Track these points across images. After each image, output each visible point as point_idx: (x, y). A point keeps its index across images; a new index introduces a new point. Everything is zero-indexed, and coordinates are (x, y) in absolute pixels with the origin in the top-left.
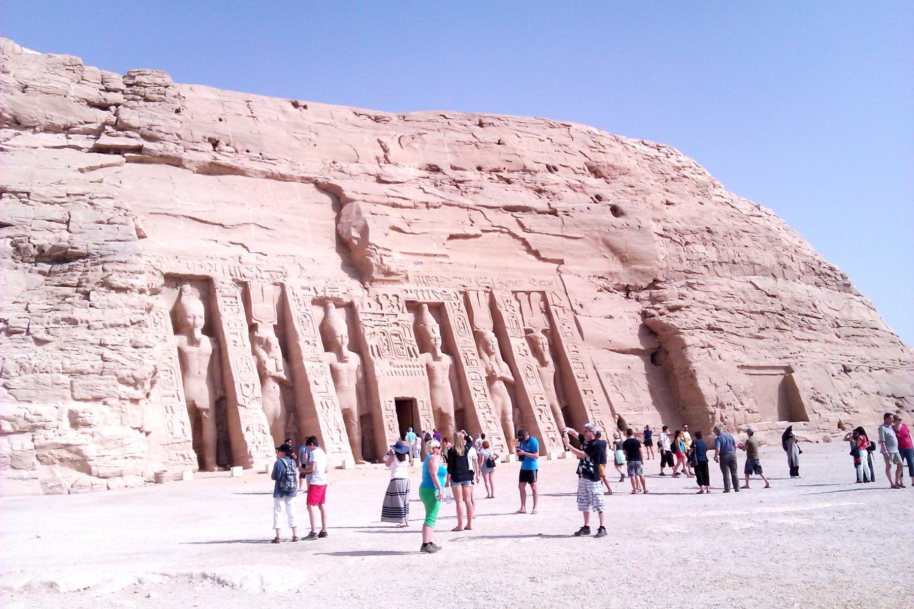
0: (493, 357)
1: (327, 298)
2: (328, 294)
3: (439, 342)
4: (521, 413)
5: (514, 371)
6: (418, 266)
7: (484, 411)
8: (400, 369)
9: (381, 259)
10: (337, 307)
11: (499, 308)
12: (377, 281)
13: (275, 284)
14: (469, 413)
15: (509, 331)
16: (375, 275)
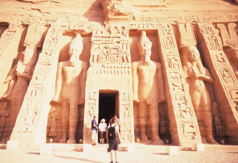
0: (195, 63)
1: (75, 30)
2: (76, 28)
3: (149, 53)
4: (219, 105)
5: (213, 73)
6: (144, 13)
7: (181, 102)
8: (109, 70)
9: (114, 5)
10: (83, 36)
11: (201, 32)
12: (111, 19)
13: (46, 26)
14: (168, 103)
15: (208, 46)
16: (110, 16)
